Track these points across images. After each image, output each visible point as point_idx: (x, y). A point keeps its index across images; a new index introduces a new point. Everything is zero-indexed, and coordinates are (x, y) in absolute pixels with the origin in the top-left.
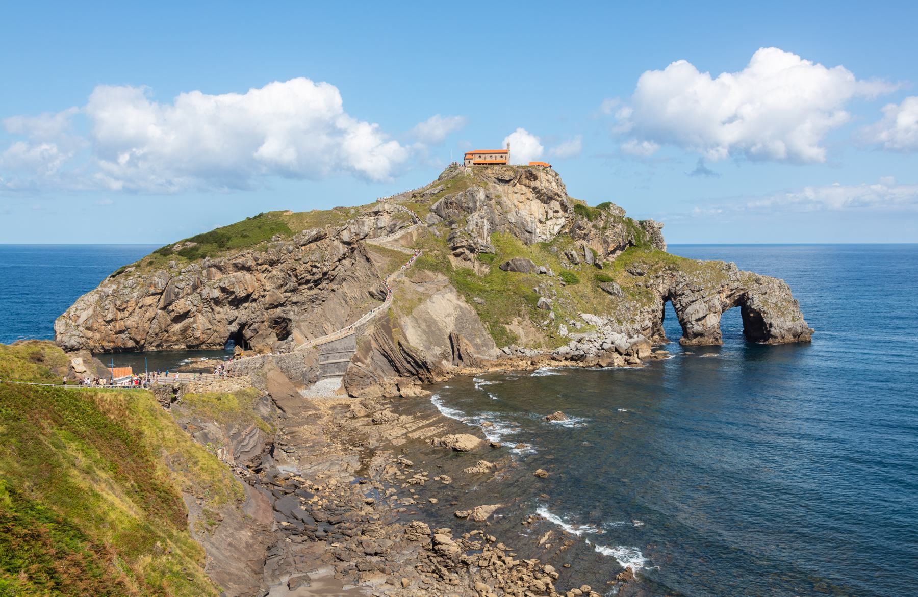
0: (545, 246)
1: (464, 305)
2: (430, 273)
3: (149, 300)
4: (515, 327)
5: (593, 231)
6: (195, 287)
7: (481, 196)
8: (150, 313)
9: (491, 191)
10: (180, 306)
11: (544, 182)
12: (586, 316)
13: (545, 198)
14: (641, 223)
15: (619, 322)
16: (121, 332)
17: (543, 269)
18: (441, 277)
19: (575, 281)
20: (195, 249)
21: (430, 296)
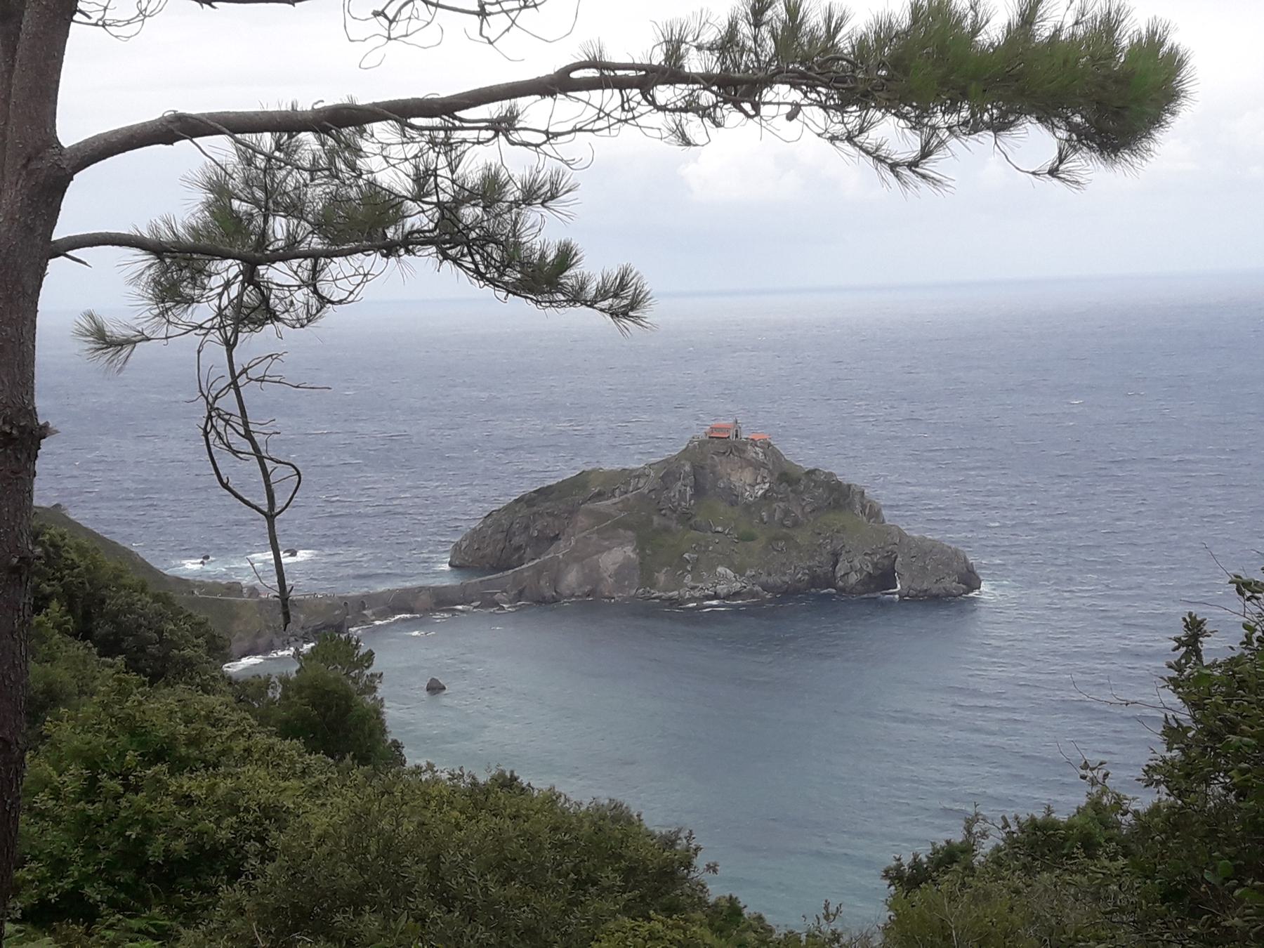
0: (748, 506)
1: (633, 556)
2: (621, 531)
3: (499, 536)
4: (661, 577)
5: (792, 495)
6: (527, 528)
7: (687, 468)
8: (501, 546)
9: (709, 461)
10: (517, 541)
11: (751, 452)
12: (720, 569)
13: (756, 466)
14: (849, 486)
15: (770, 574)
16: (483, 557)
17: (720, 529)
18: (630, 533)
19: (752, 538)
20: (534, 499)
21: (609, 549)
